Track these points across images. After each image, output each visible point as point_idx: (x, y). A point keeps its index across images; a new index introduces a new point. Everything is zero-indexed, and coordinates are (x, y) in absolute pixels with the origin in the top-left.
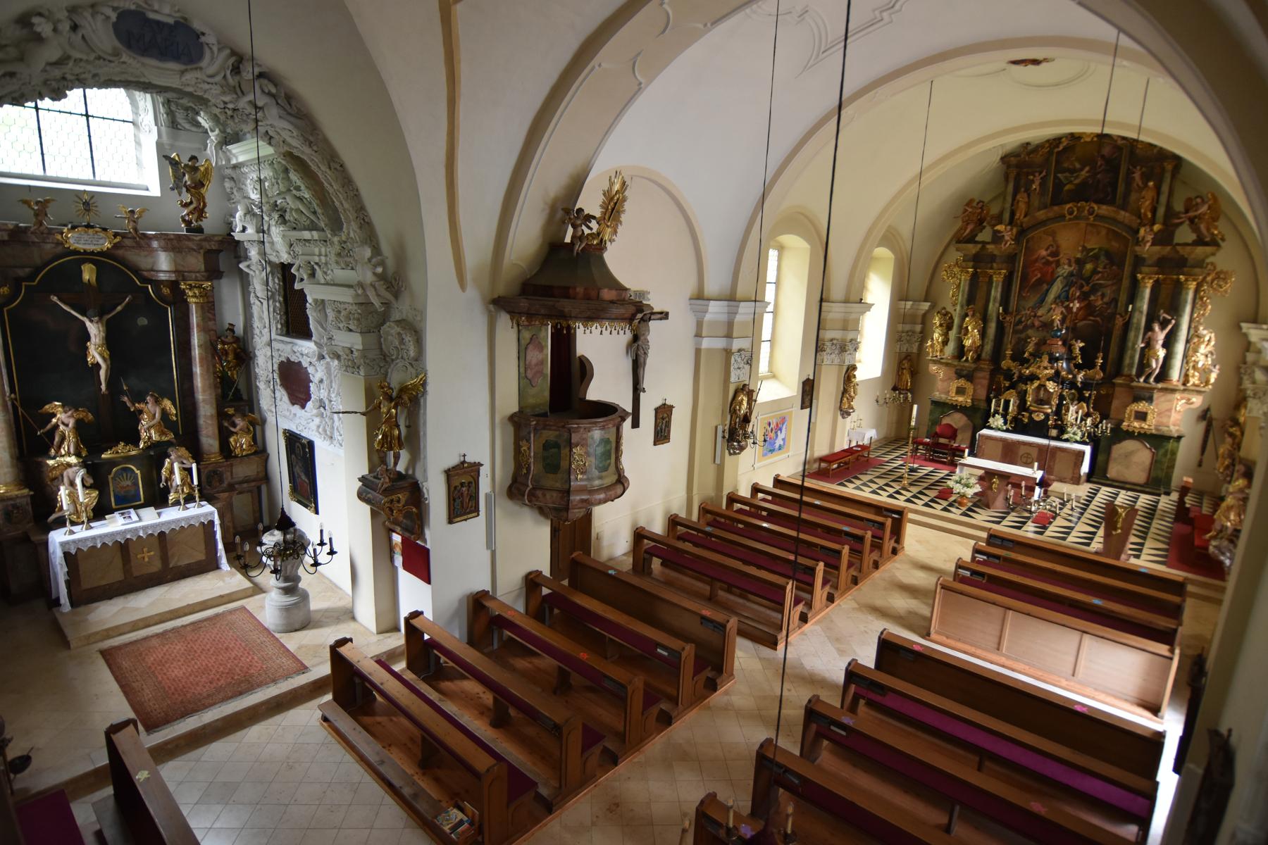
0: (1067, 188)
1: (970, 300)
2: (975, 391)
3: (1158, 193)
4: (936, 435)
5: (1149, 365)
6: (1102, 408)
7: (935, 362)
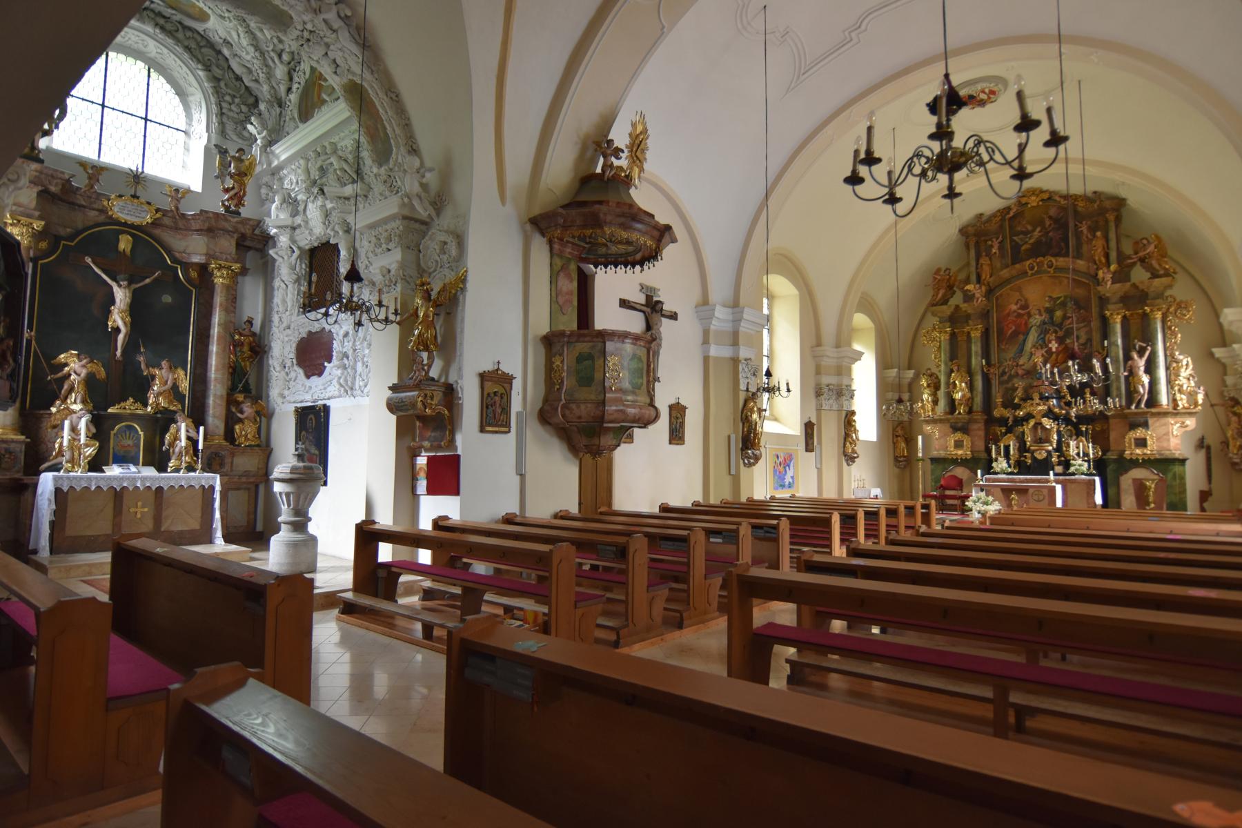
1: (953, 356)
3: (1107, 240)
4: (944, 488)
5: (1137, 392)
6: (1100, 439)
7: (928, 422)
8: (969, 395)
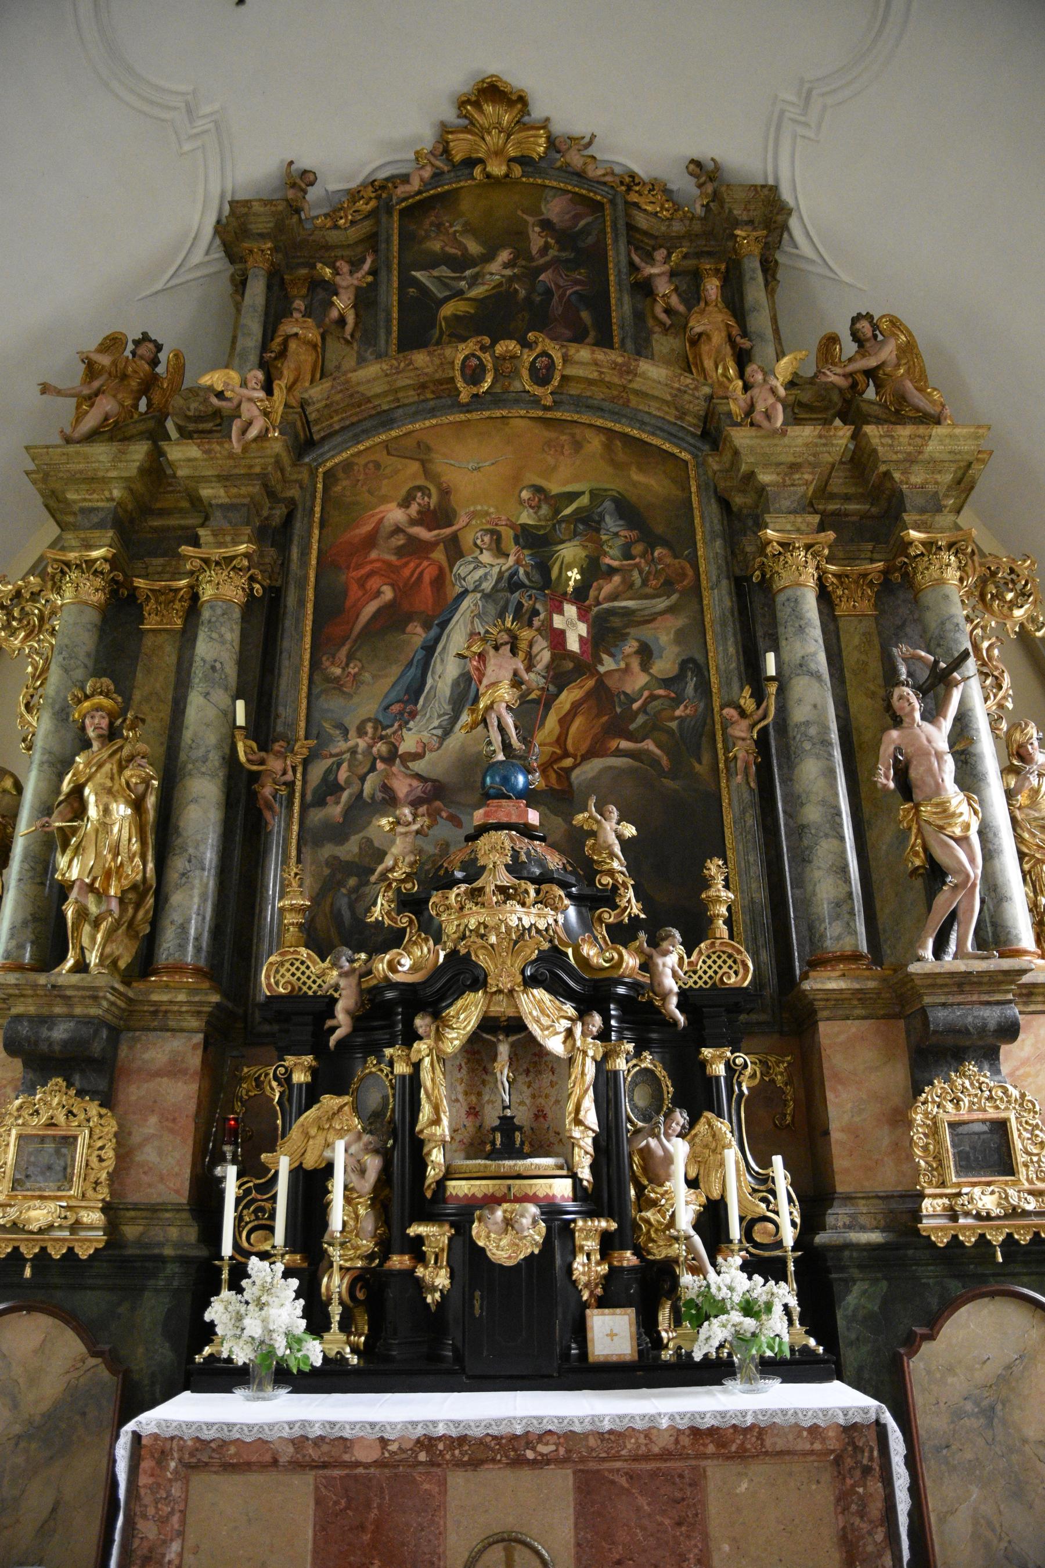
0: (448, 310)
6: (791, 1126)
8: (138, 868)
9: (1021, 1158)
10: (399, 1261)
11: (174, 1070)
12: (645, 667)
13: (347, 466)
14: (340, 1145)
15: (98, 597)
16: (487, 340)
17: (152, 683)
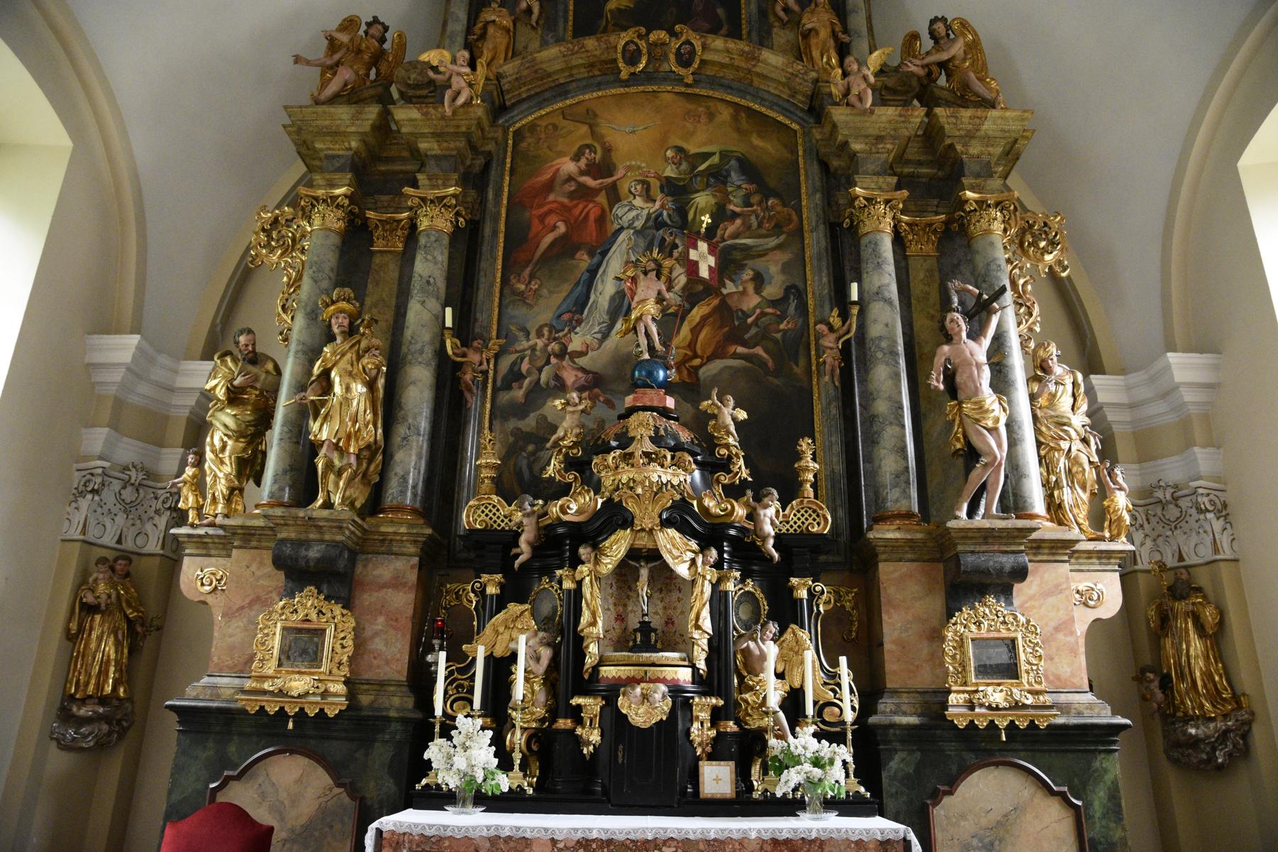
2: (360, 643)
6: (855, 637)
8: (372, 434)
9: (1024, 667)
10: (564, 723)
11: (396, 583)
12: (758, 290)
13: (532, 127)
14: (522, 639)
15: (340, 225)
16: (643, 30)
17: (381, 291)
